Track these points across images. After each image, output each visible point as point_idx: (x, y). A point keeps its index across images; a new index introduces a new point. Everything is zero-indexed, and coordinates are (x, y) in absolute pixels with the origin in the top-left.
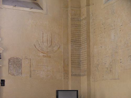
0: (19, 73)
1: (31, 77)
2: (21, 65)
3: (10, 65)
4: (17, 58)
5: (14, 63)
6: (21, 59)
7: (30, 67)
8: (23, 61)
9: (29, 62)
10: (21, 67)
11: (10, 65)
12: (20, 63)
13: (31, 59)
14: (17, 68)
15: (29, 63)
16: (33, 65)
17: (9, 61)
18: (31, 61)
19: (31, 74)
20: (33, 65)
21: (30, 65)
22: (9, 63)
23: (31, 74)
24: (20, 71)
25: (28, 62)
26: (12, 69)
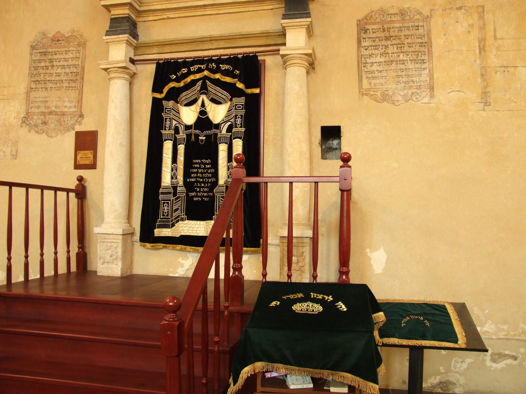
0: (419, 88)
1: (486, 104)
2: (428, 44)
3: (367, 53)
4: (402, 13)
5: (387, 38)
6: (426, 12)
7: (482, 49)
8: (436, 24)
9: (471, 26)
10: (430, 53)
11: (367, 53)
12: (422, 36)
13: (483, 7)
14: (403, 62)
15: (476, 32)
16: (495, 38)
17: (362, 28)
18: (488, 17)
19: (486, 87)
20: (495, 38)
21: (482, 41)
22: (359, 42)
23: (486, 87)
24: (425, 75)
25: (465, 24)
26: (375, 67)
